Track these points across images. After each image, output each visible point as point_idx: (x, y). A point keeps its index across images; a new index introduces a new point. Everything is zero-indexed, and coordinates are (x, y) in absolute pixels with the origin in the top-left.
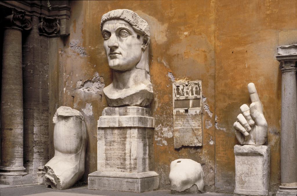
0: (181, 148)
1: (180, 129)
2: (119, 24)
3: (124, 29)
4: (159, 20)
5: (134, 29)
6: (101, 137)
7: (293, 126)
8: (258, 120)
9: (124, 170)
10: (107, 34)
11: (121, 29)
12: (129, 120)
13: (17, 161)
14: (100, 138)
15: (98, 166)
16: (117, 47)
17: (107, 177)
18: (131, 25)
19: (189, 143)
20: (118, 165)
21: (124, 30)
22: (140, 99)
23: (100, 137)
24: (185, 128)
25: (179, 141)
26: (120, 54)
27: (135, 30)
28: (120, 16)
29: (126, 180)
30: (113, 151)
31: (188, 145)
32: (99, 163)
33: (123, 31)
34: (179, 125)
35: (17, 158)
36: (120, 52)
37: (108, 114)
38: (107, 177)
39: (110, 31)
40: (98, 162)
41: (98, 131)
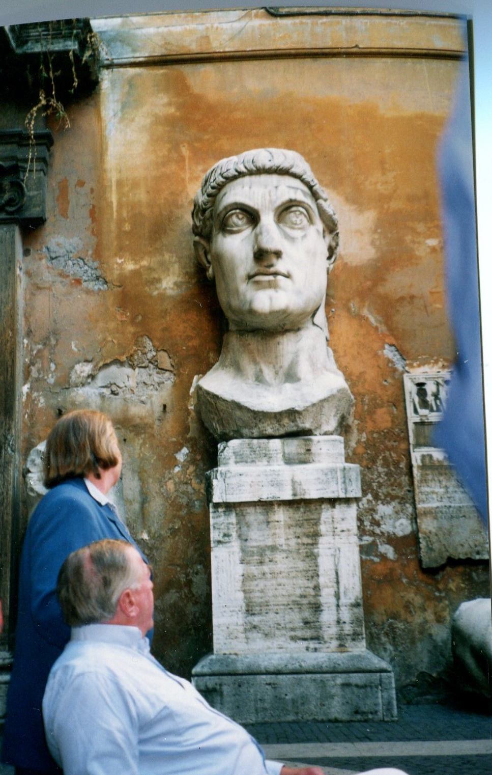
0: (442, 568)
1: (438, 507)
2: (287, 189)
3: (298, 204)
4: (347, 200)
6: (225, 535)
9: (317, 646)
10: (240, 216)
11: (294, 203)
12: (329, 476)
14: (221, 539)
15: (215, 637)
16: (278, 254)
17: (267, 673)
18: (315, 196)
19: (470, 550)
20: (293, 629)
21: (301, 209)
23: (222, 535)
24: (453, 505)
25: (436, 546)
26: (288, 276)
27: (322, 212)
29: (340, 679)
30: (274, 582)
31: (469, 556)
32: (219, 626)
33: (296, 211)
34: (434, 496)
36: (288, 273)
37: (241, 459)
38: (267, 673)
39: (256, 207)
40: (215, 621)
41: (211, 515)
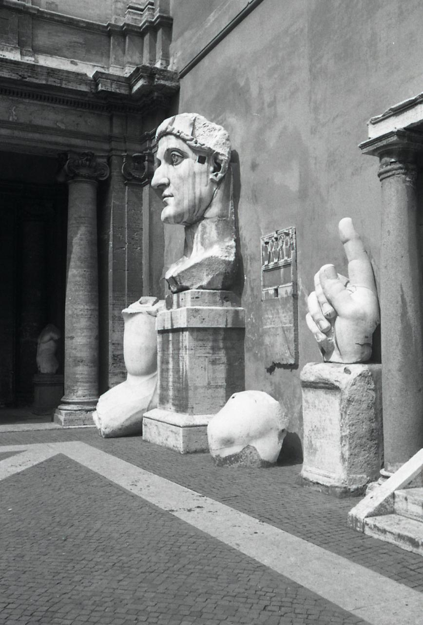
5: (190, 147)
7: (396, 315)
8: (335, 304)
13: (80, 388)
21: (174, 153)
22: (207, 275)
26: (172, 196)
28: (167, 129)
35: (81, 382)
